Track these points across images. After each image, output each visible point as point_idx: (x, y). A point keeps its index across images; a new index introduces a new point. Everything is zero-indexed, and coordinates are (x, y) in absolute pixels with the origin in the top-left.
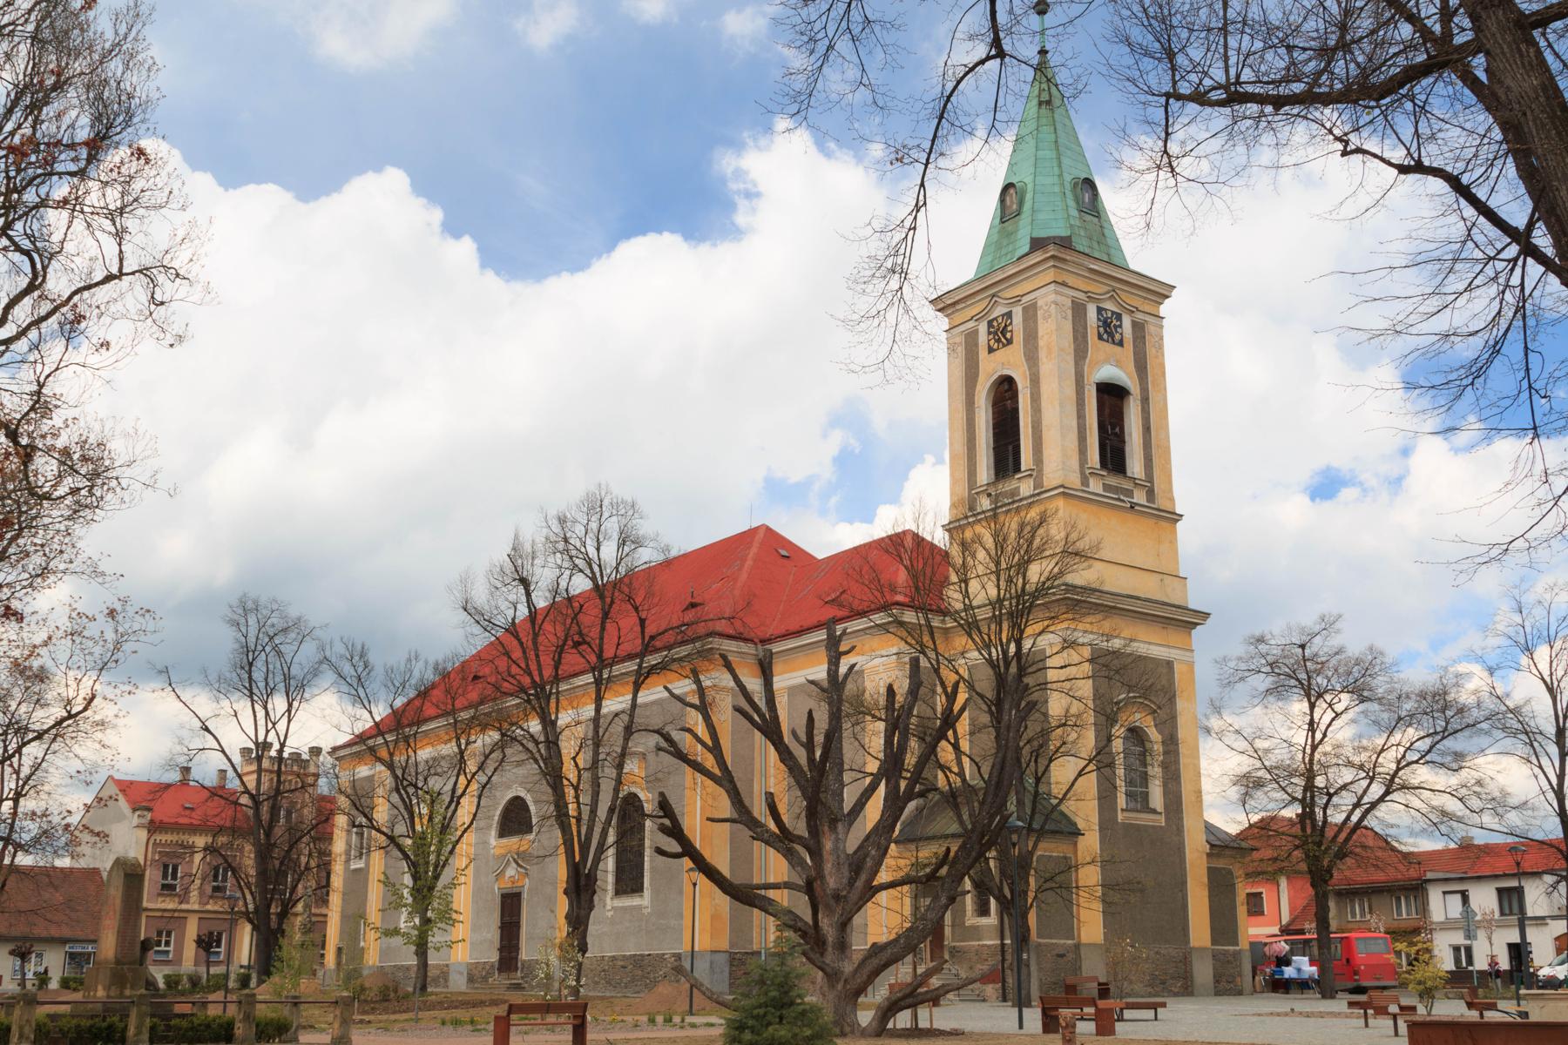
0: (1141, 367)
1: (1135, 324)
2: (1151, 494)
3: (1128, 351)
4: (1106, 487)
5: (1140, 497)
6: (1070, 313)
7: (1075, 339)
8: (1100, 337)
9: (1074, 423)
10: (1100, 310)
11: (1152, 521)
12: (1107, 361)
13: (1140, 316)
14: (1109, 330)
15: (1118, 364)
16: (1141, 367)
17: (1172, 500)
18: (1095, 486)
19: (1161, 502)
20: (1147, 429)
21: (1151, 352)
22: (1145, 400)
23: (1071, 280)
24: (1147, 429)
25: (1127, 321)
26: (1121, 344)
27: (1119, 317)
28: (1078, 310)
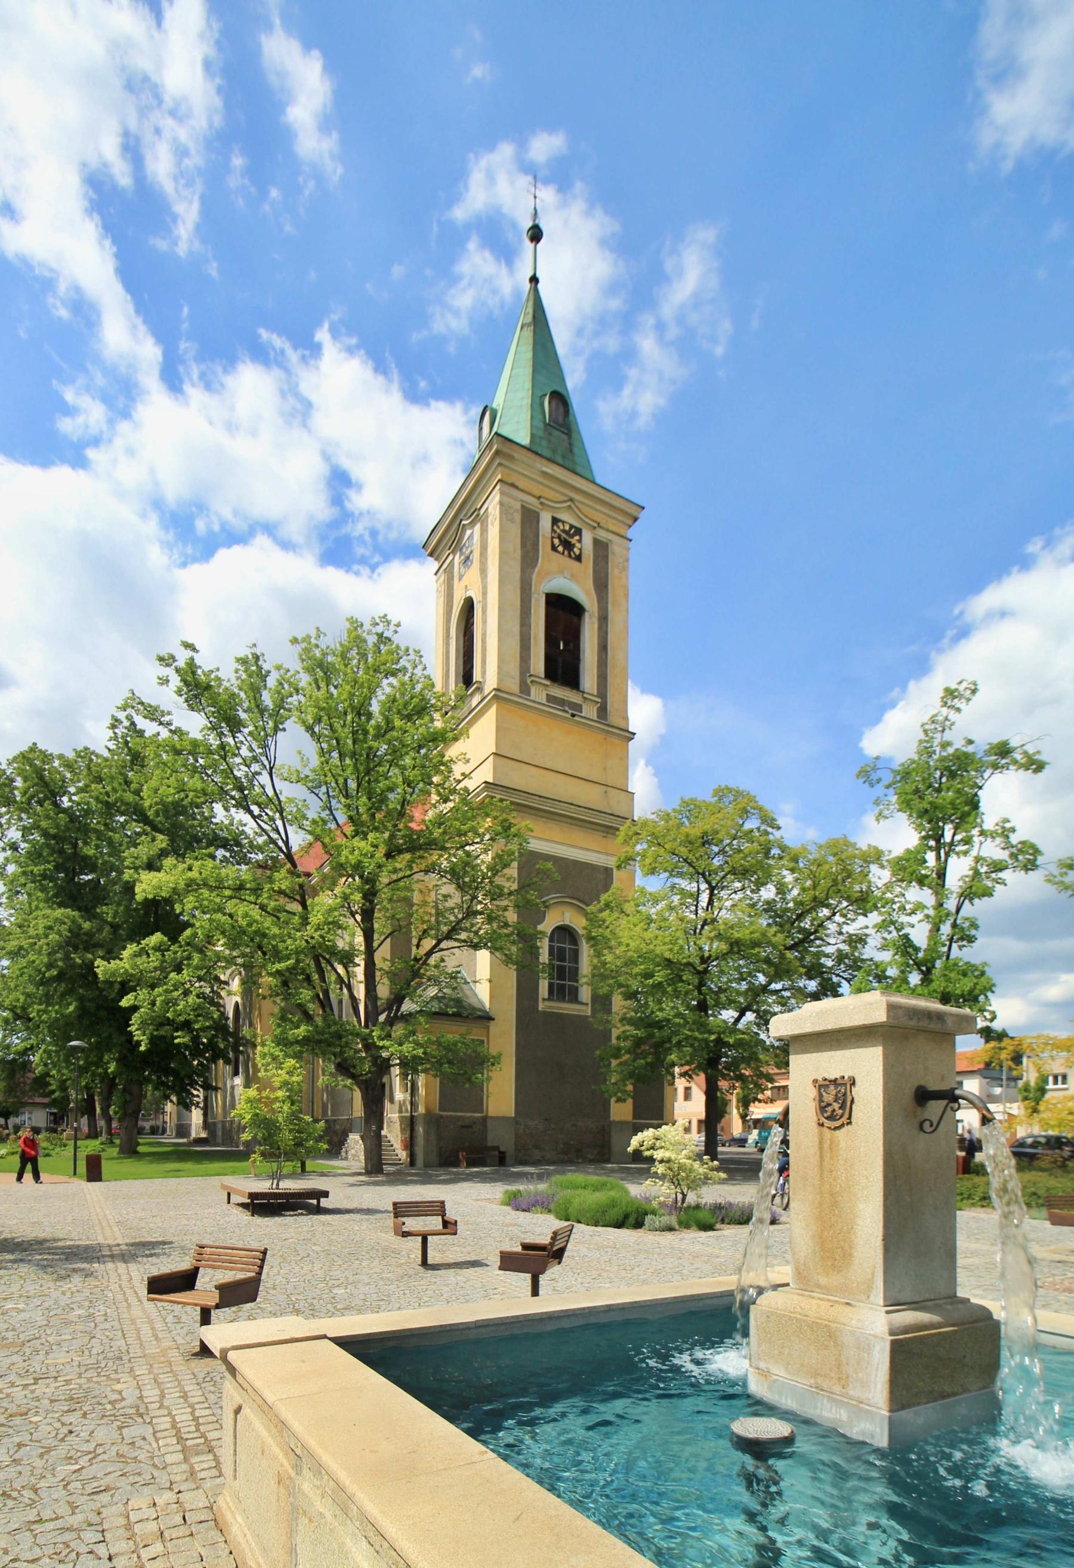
0: (601, 585)
1: (597, 543)
2: (603, 711)
4: (550, 699)
5: (590, 711)
6: (518, 517)
7: (523, 545)
8: (554, 548)
9: (517, 629)
10: (555, 521)
12: (561, 572)
13: (602, 535)
15: (573, 577)
16: (601, 585)
17: (627, 719)
18: (538, 694)
19: (614, 719)
20: (603, 647)
21: (614, 572)
22: (603, 619)
23: (521, 484)
24: (603, 647)
25: (587, 537)
26: (578, 558)
27: (579, 532)
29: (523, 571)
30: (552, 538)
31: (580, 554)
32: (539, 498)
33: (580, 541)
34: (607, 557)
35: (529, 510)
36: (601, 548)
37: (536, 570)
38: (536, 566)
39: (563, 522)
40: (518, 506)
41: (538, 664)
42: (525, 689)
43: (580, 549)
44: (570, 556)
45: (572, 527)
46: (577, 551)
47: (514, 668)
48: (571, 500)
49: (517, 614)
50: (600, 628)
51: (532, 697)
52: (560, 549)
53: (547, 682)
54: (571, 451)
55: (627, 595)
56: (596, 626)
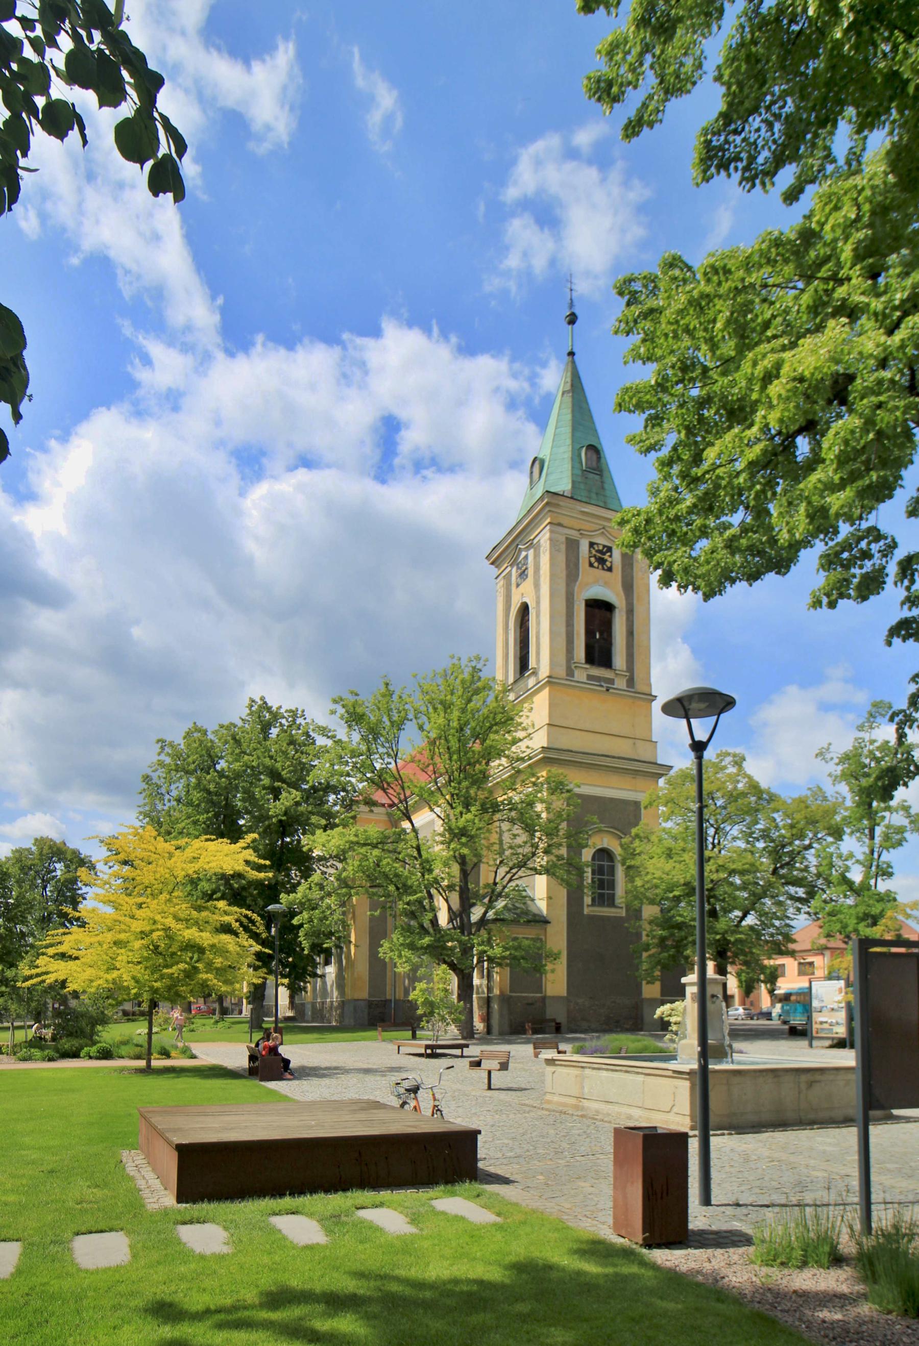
0: (628, 587)
2: (631, 682)
4: (590, 677)
5: (620, 683)
7: (568, 566)
8: (591, 565)
9: (563, 630)
10: (592, 545)
15: (606, 584)
16: (628, 587)
17: (650, 685)
19: (640, 687)
20: (630, 633)
22: (630, 612)
24: (630, 633)
26: (610, 569)
27: (610, 549)
28: (572, 545)
29: (568, 585)
41: (580, 653)
42: (570, 673)
45: (604, 546)
46: (608, 564)
47: (562, 658)
52: (596, 564)
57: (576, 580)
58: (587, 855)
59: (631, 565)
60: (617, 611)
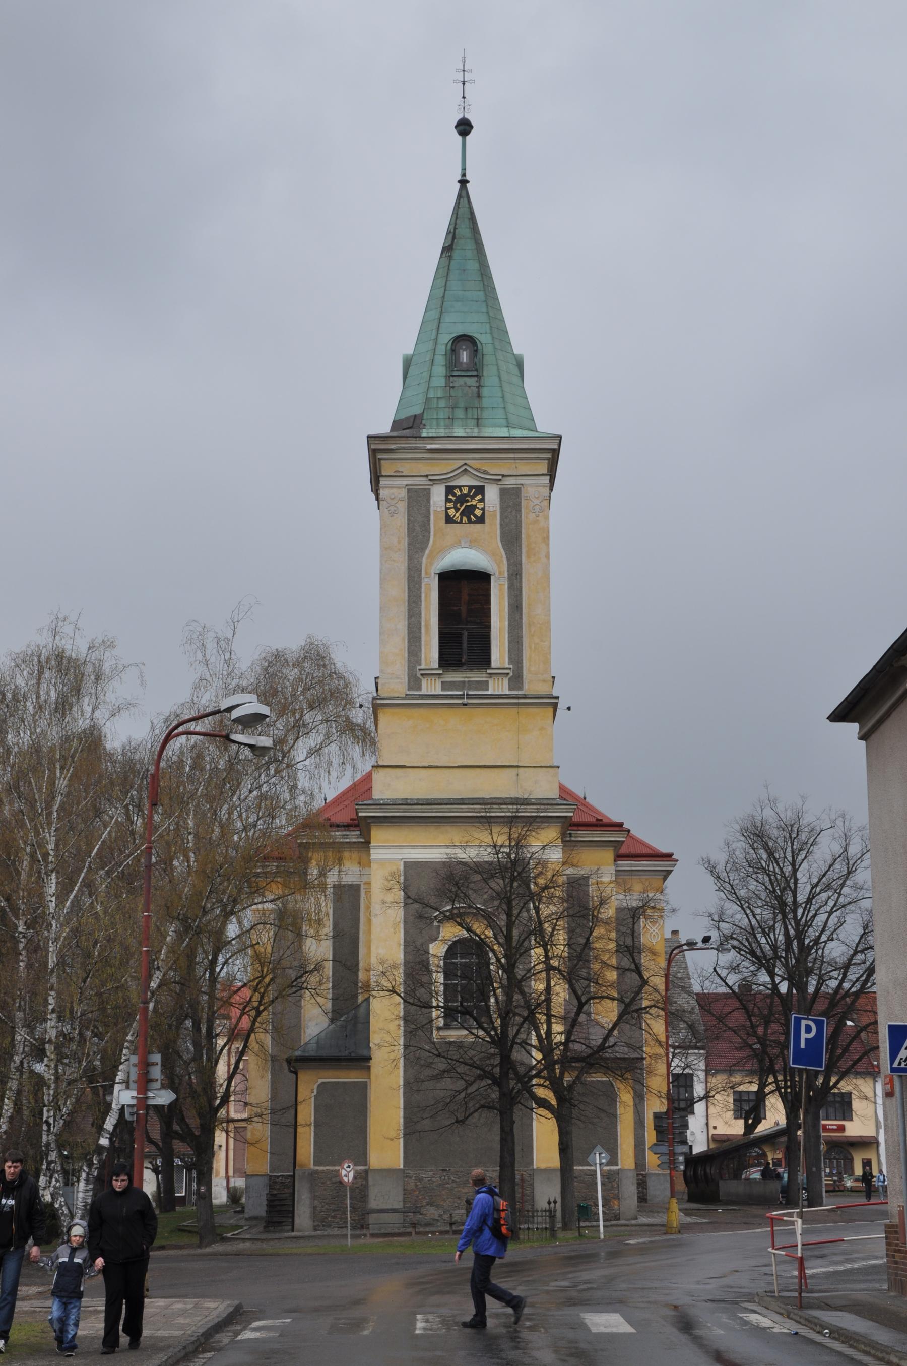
0: (512, 539)
1: (505, 494)
2: (516, 679)
3: (493, 527)
4: (445, 685)
6: (402, 507)
7: (411, 530)
8: (449, 520)
10: (449, 490)
11: (514, 710)
12: (457, 544)
13: (510, 482)
14: (465, 507)
15: (473, 543)
16: (512, 539)
19: (532, 685)
20: (516, 607)
21: (527, 517)
22: (515, 575)
24: (516, 607)
25: (492, 494)
26: (481, 520)
27: (480, 490)
28: (418, 499)
29: (410, 558)
30: (447, 509)
31: (483, 514)
32: (427, 476)
33: (482, 500)
34: (520, 504)
35: (416, 490)
36: (512, 499)
37: (427, 552)
38: (426, 547)
39: (460, 487)
40: (403, 493)
42: (414, 681)
43: (483, 509)
44: (470, 521)
45: (471, 488)
46: (478, 512)
48: (465, 464)
49: (403, 609)
50: (511, 587)
51: (424, 692)
53: (441, 672)
54: (479, 396)
55: (546, 539)
56: (506, 586)
57: (423, 550)
58: (437, 949)
59: (517, 507)
60: (492, 577)
